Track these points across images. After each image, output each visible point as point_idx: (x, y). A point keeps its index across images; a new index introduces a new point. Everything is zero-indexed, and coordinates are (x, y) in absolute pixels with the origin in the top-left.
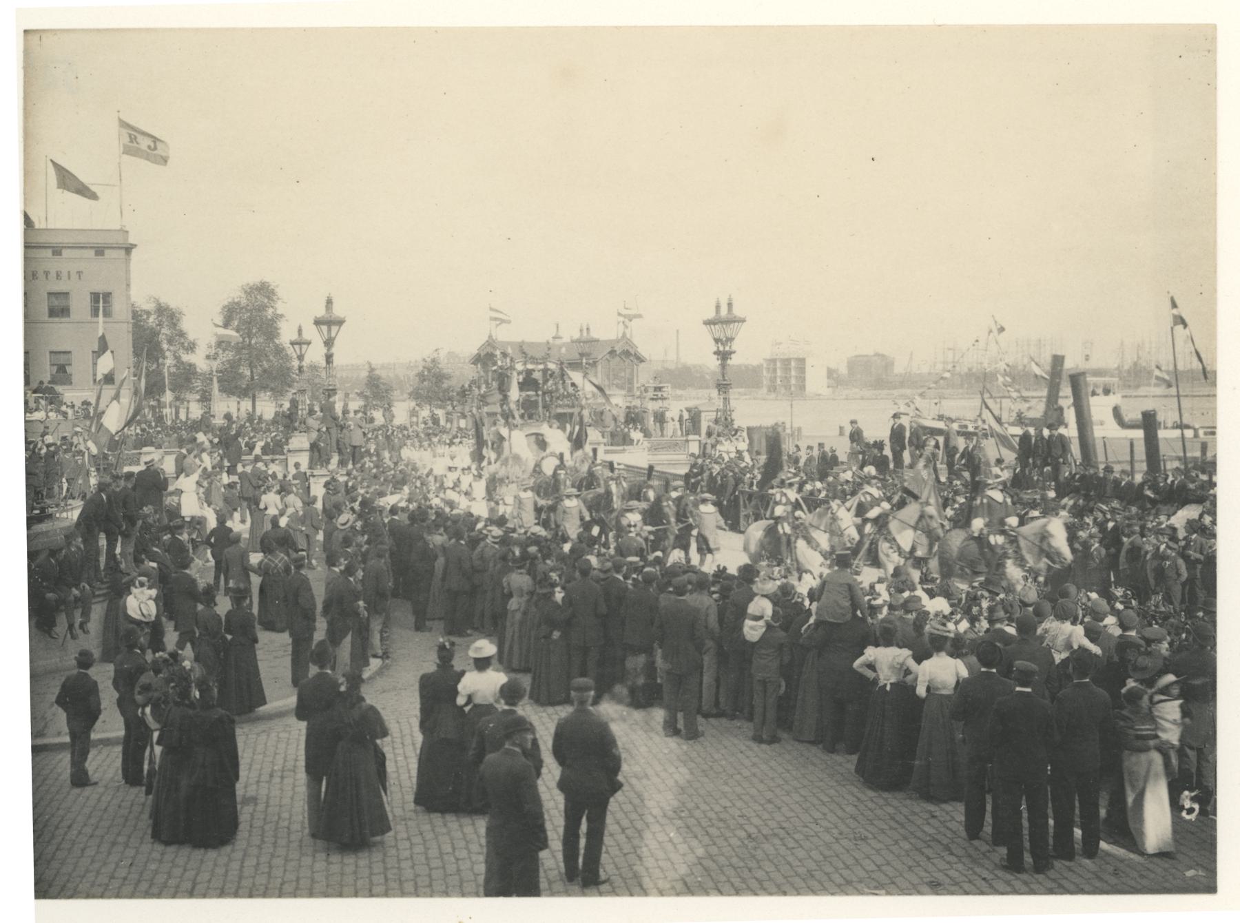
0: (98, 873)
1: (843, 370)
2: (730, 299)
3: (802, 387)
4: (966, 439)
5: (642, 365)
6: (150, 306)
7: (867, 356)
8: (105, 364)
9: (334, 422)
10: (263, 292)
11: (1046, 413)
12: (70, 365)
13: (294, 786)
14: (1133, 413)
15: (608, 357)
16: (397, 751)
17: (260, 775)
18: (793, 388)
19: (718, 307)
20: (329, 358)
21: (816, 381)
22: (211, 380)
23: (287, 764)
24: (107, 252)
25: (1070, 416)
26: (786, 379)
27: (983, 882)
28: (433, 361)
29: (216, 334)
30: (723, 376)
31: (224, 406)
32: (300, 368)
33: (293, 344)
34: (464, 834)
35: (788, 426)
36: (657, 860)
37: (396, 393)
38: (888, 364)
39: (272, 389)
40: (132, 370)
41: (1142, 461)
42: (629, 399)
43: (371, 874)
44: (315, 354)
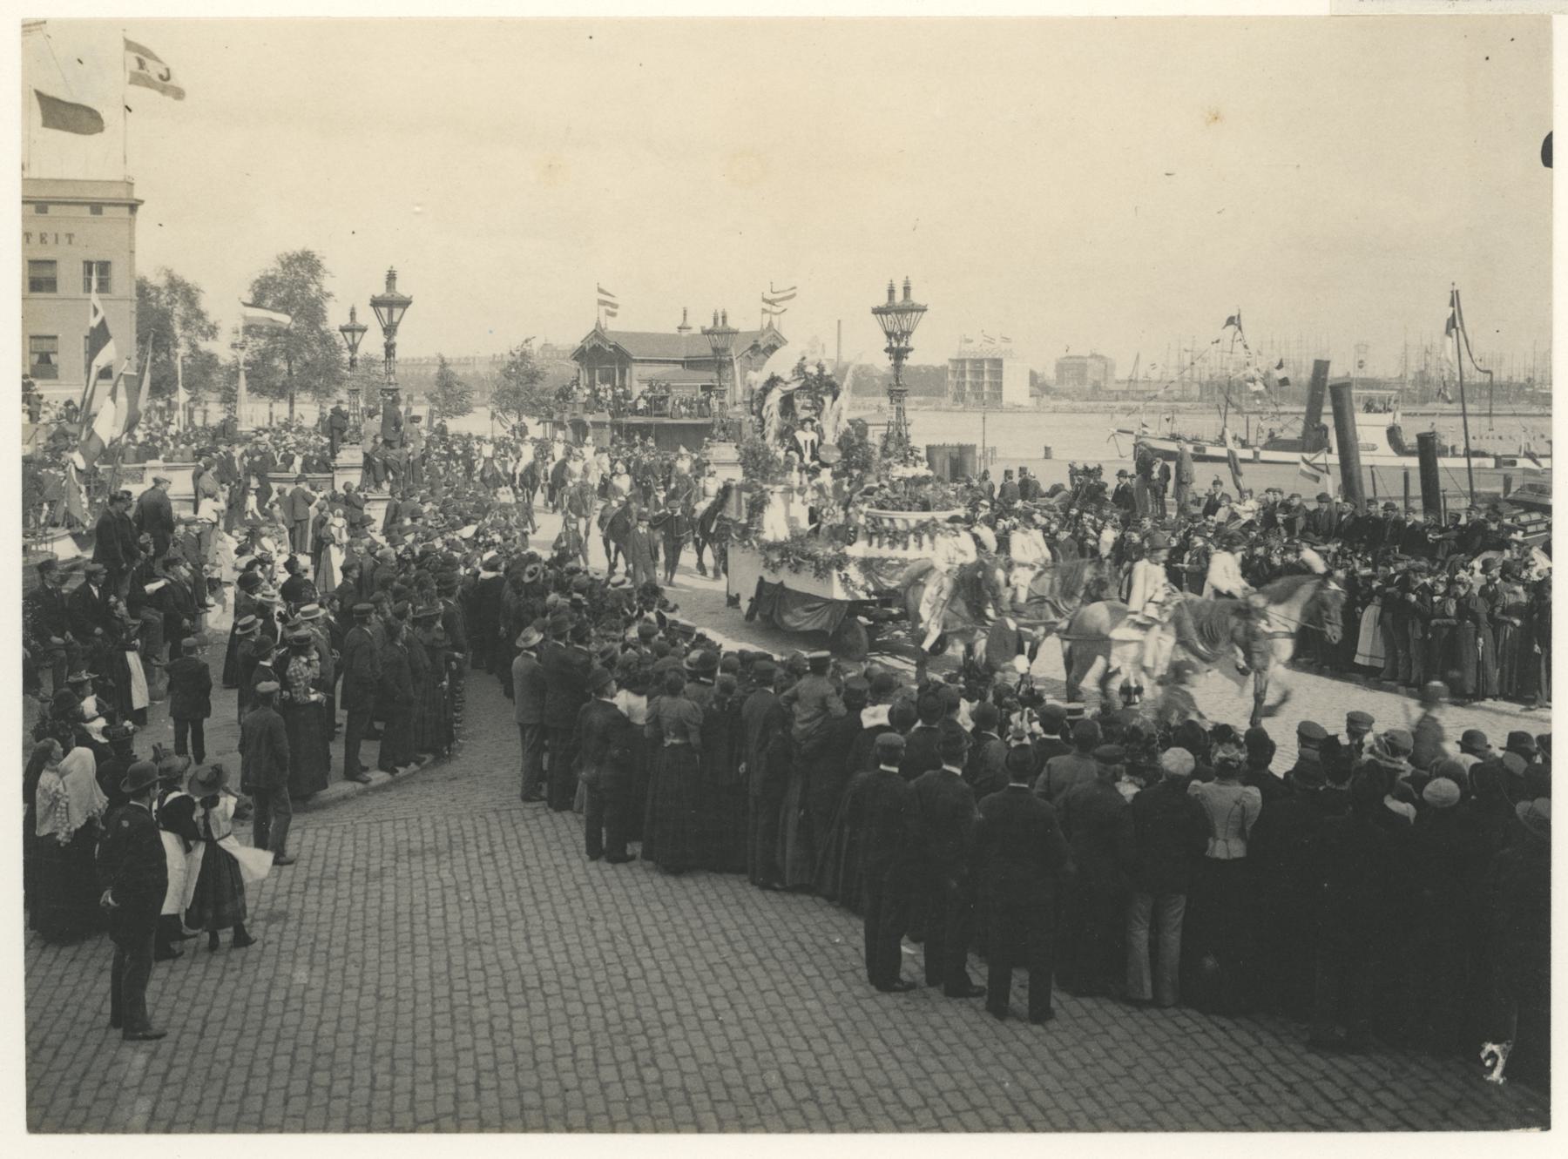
0: (81, 1007)
2: (907, 282)
3: (997, 395)
7: (1082, 357)
10: (305, 264)
12: (55, 353)
13: (336, 899)
14: (1410, 440)
15: (749, 353)
16: (469, 855)
17: (291, 885)
18: (986, 397)
19: (891, 292)
20: (390, 349)
21: (1015, 389)
22: (238, 376)
23: (327, 869)
24: (105, 210)
26: (977, 386)
27: (1222, 1034)
28: (523, 354)
29: (245, 318)
30: (897, 380)
31: (254, 413)
32: (353, 362)
33: (343, 330)
34: (555, 964)
35: (979, 445)
37: (476, 395)
38: (1107, 366)
39: (316, 388)
40: (135, 361)
41: (1417, 498)
43: (434, 1013)
44: (371, 344)
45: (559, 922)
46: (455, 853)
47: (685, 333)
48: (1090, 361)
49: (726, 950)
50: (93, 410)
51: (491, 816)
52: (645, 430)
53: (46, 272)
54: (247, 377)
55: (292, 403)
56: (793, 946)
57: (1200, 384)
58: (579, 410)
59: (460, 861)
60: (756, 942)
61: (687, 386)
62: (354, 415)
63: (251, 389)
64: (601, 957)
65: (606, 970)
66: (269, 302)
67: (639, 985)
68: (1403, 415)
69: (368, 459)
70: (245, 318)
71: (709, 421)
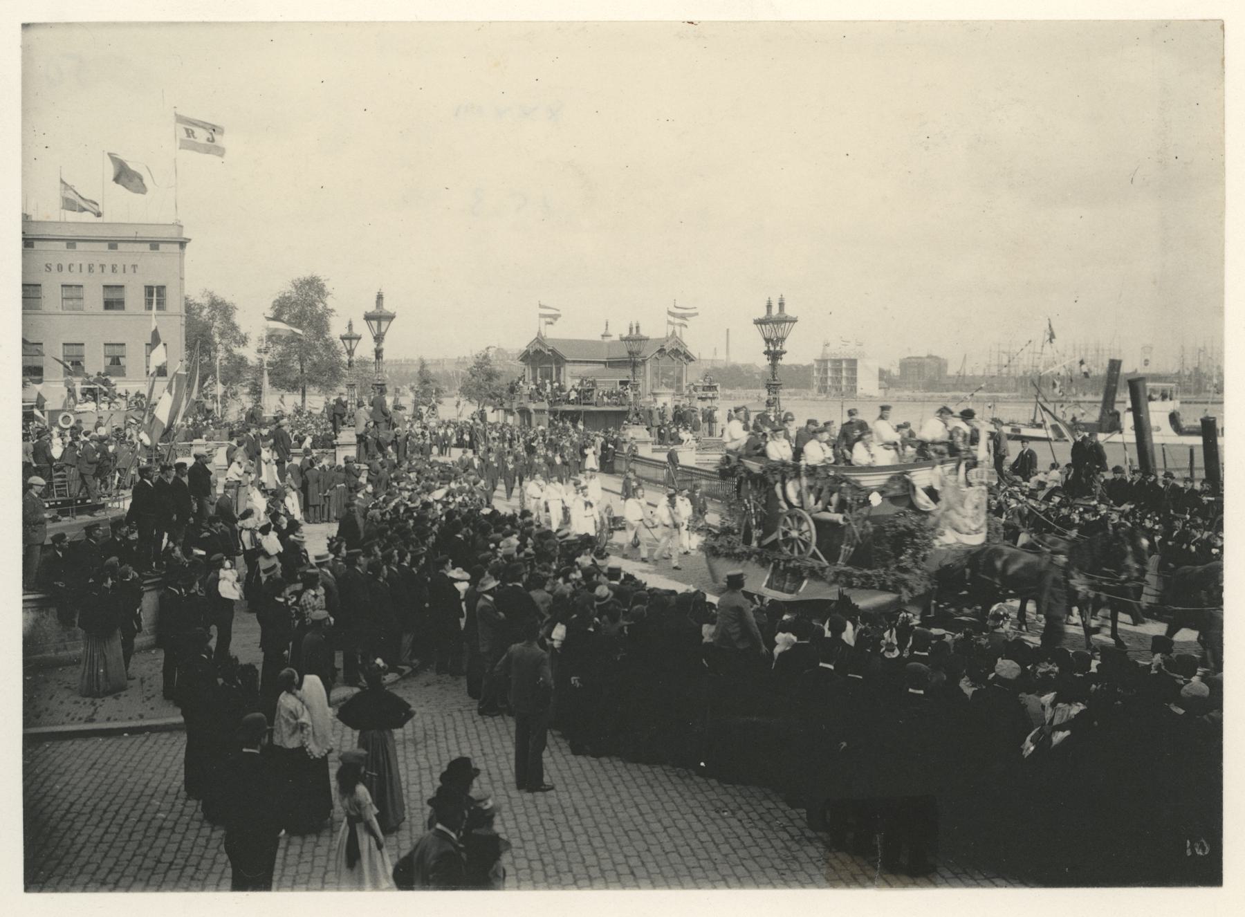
0: (145, 856)
1: (895, 371)
2: (781, 299)
4: (1023, 442)
5: (692, 364)
6: (205, 301)
8: (158, 357)
9: (383, 417)
10: (312, 288)
11: (1101, 418)
12: (124, 356)
14: (1191, 419)
15: (657, 355)
18: (844, 389)
19: (769, 306)
20: (378, 353)
22: (262, 374)
24: (162, 246)
25: (1128, 420)
29: (268, 329)
30: (774, 377)
31: (275, 402)
32: (350, 363)
33: (343, 338)
36: (699, 860)
38: (941, 364)
41: (1200, 469)
42: (678, 398)
45: (509, 797)
46: (429, 742)
47: (607, 340)
48: (928, 360)
49: (639, 820)
50: (152, 401)
51: (456, 714)
52: (574, 417)
53: (114, 296)
54: (269, 374)
55: (304, 394)
56: (690, 817)
57: (1016, 380)
58: (524, 400)
59: (433, 749)
60: (662, 814)
61: (608, 381)
62: (351, 404)
63: (273, 384)
64: (542, 824)
65: (545, 834)
66: (286, 317)
67: (570, 846)
68: (1181, 403)
69: (361, 438)
70: (268, 329)
71: (626, 408)
